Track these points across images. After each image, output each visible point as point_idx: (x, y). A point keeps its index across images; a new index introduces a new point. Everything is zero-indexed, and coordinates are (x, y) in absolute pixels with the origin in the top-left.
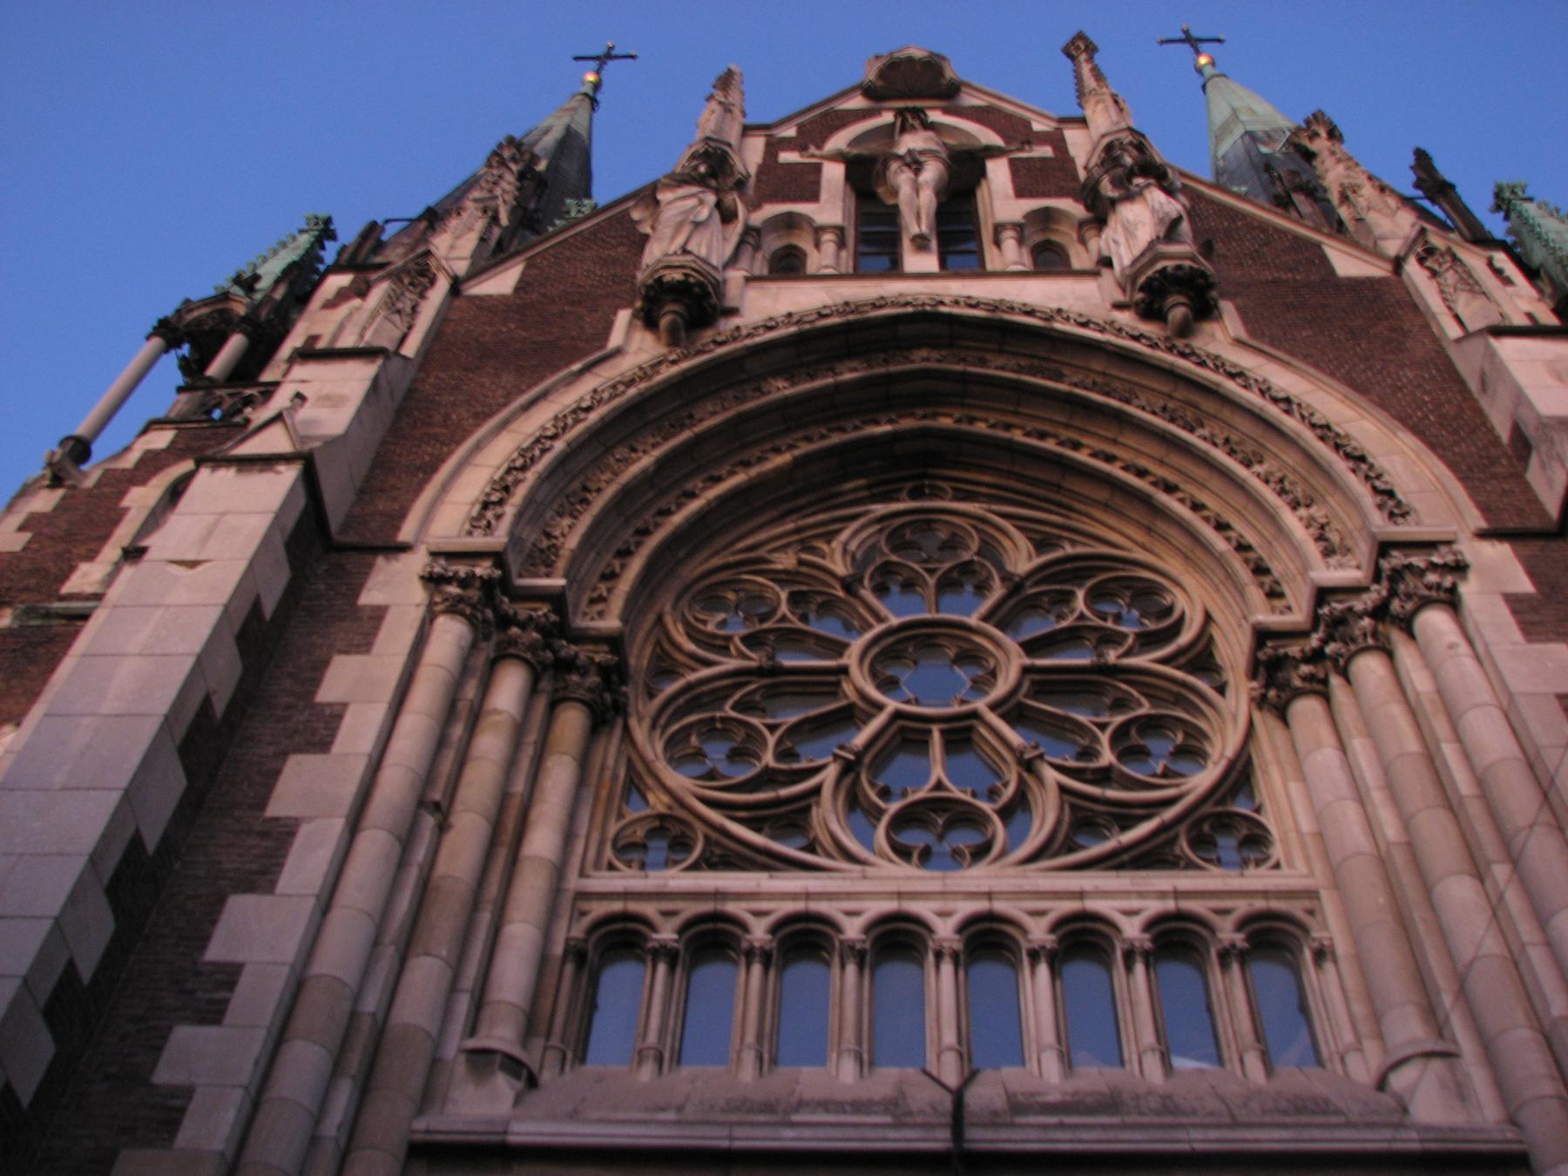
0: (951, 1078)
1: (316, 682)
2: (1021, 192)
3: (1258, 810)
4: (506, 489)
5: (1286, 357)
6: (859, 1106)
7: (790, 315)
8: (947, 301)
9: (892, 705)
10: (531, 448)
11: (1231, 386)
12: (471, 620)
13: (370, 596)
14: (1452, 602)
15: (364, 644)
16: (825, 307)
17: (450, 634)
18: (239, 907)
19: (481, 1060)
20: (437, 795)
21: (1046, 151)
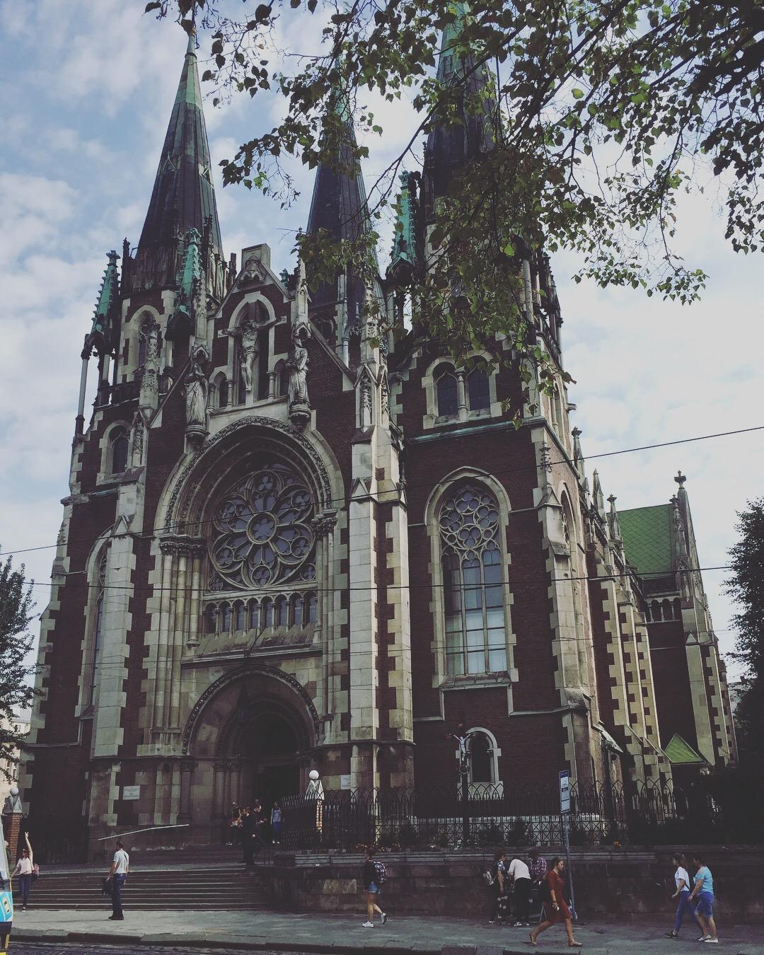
0: (258, 635)
1: (147, 579)
2: (276, 353)
3: (315, 564)
4: (170, 515)
5: (322, 438)
6: (240, 646)
7: (220, 432)
8: (252, 420)
9: (254, 542)
10: (172, 499)
11: (308, 451)
12: (170, 554)
13: (152, 553)
14: (332, 532)
15: (153, 568)
16: (227, 427)
17: (169, 558)
18: (147, 633)
19: (190, 646)
20: (173, 596)
21: (284, 321)
